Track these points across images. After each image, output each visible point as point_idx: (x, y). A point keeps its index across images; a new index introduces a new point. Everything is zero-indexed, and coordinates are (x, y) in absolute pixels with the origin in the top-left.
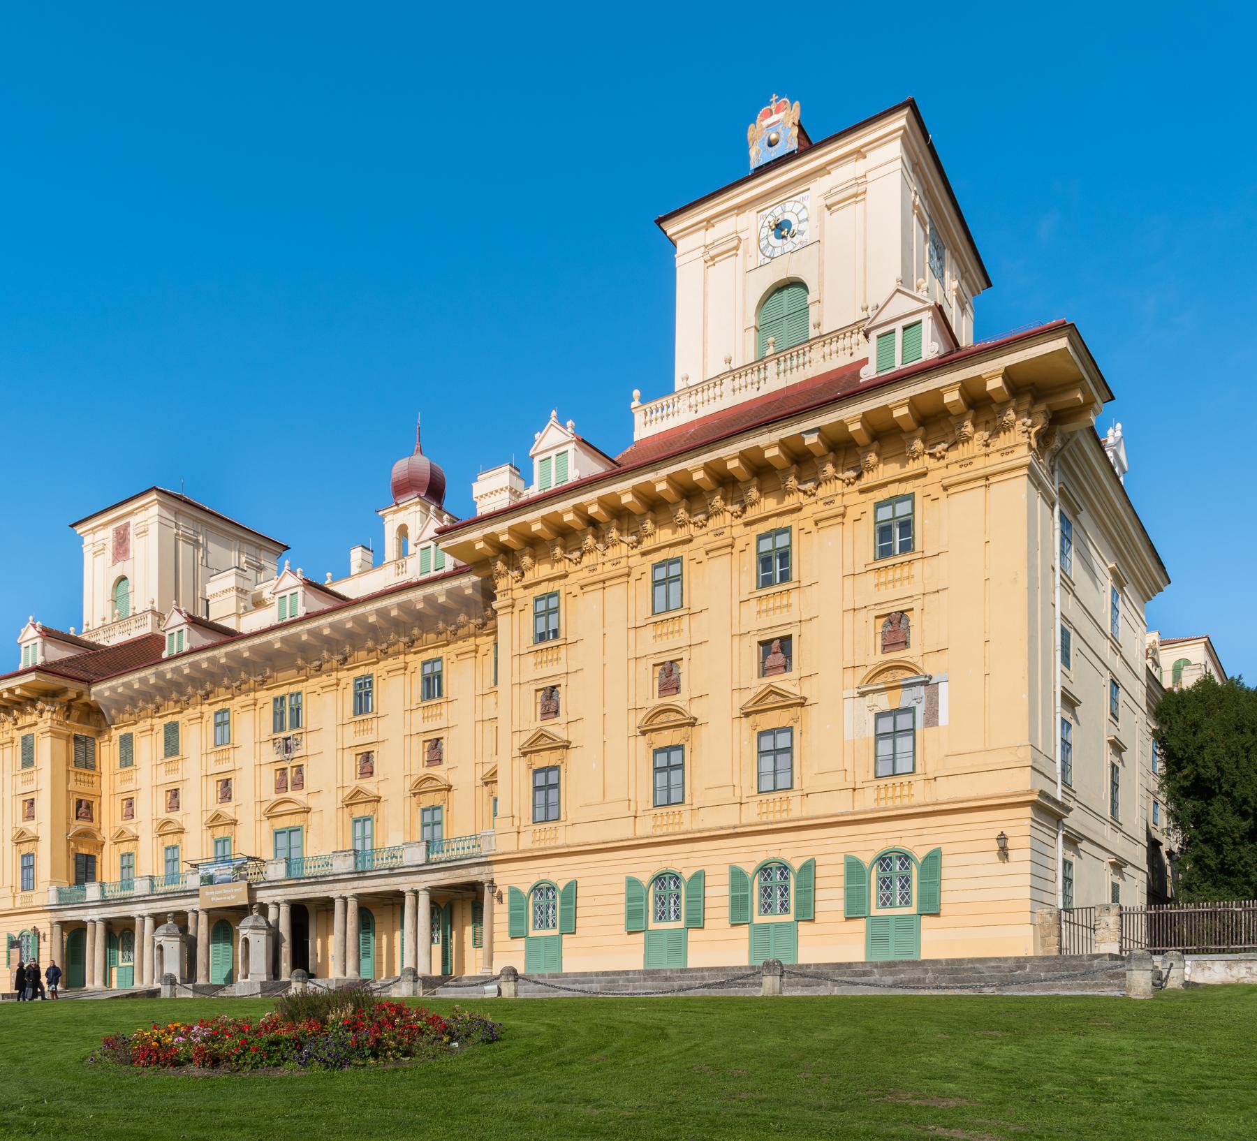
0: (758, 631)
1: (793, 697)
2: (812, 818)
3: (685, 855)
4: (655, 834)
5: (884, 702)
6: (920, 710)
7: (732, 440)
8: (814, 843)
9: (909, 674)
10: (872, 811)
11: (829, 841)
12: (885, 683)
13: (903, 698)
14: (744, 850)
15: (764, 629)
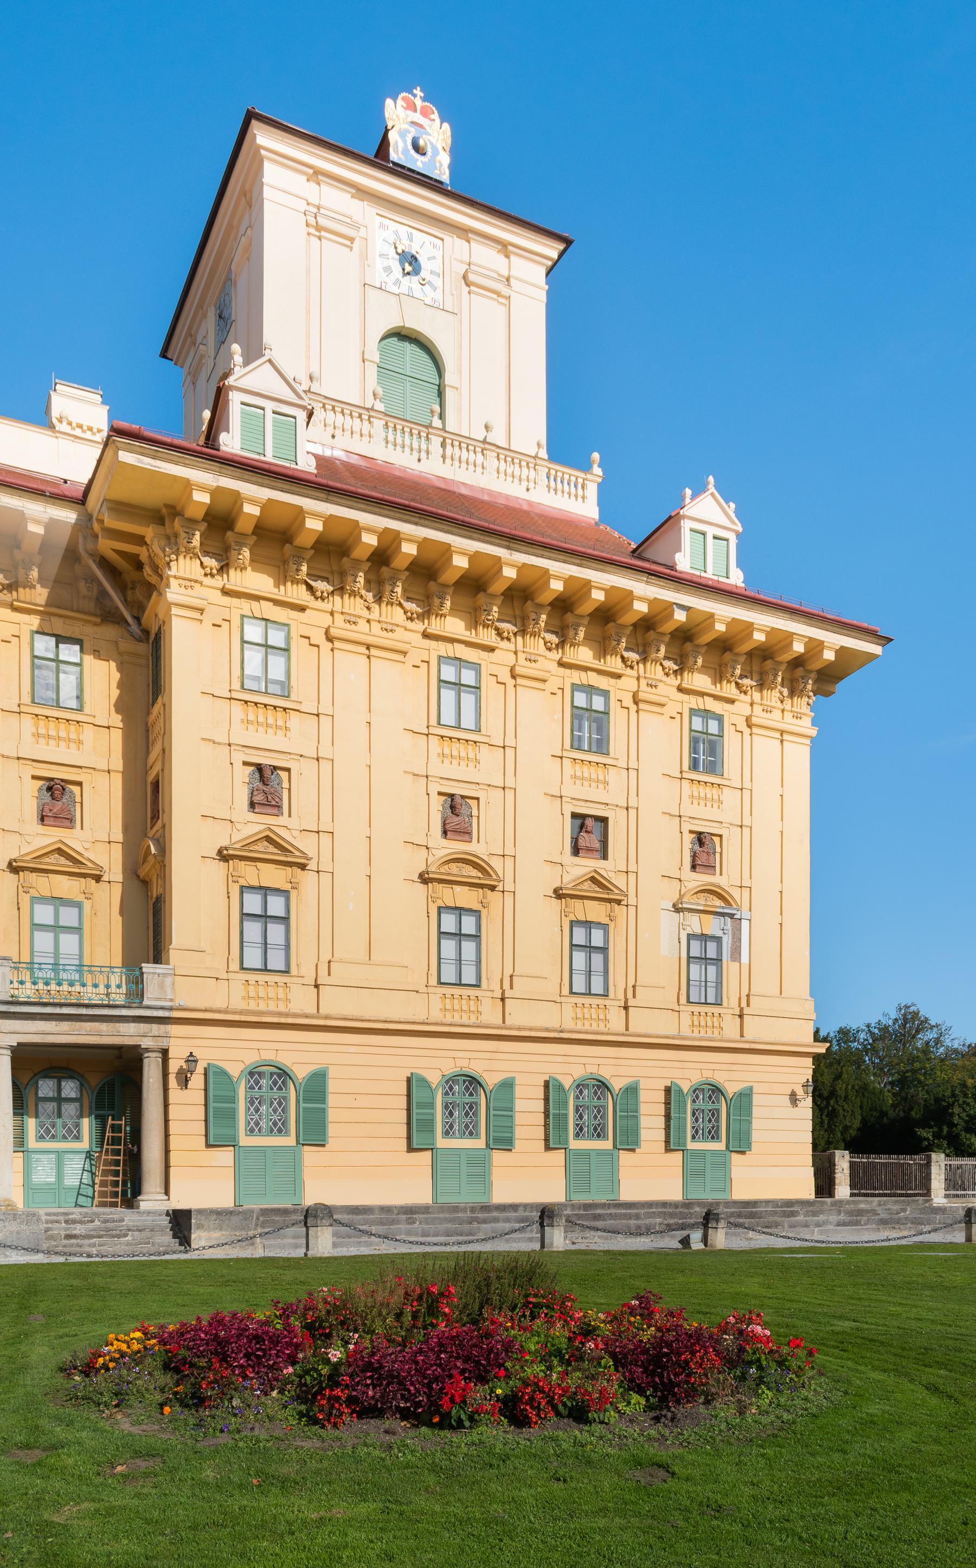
0: (572, 799)
1: (297, 853)
2: (649, 1036)
3: (488, 1055)
4: (444, 1021)
5: (695, 924)
6: (727, 942)
7: (609, 568)
8: (634, 1063)
9: (718, 902)
10: (241, 1012)
11: (650, 1063)
12: (705, 905)
13: (712, 926)
14: (559, 1059)
15: (579, 800)
